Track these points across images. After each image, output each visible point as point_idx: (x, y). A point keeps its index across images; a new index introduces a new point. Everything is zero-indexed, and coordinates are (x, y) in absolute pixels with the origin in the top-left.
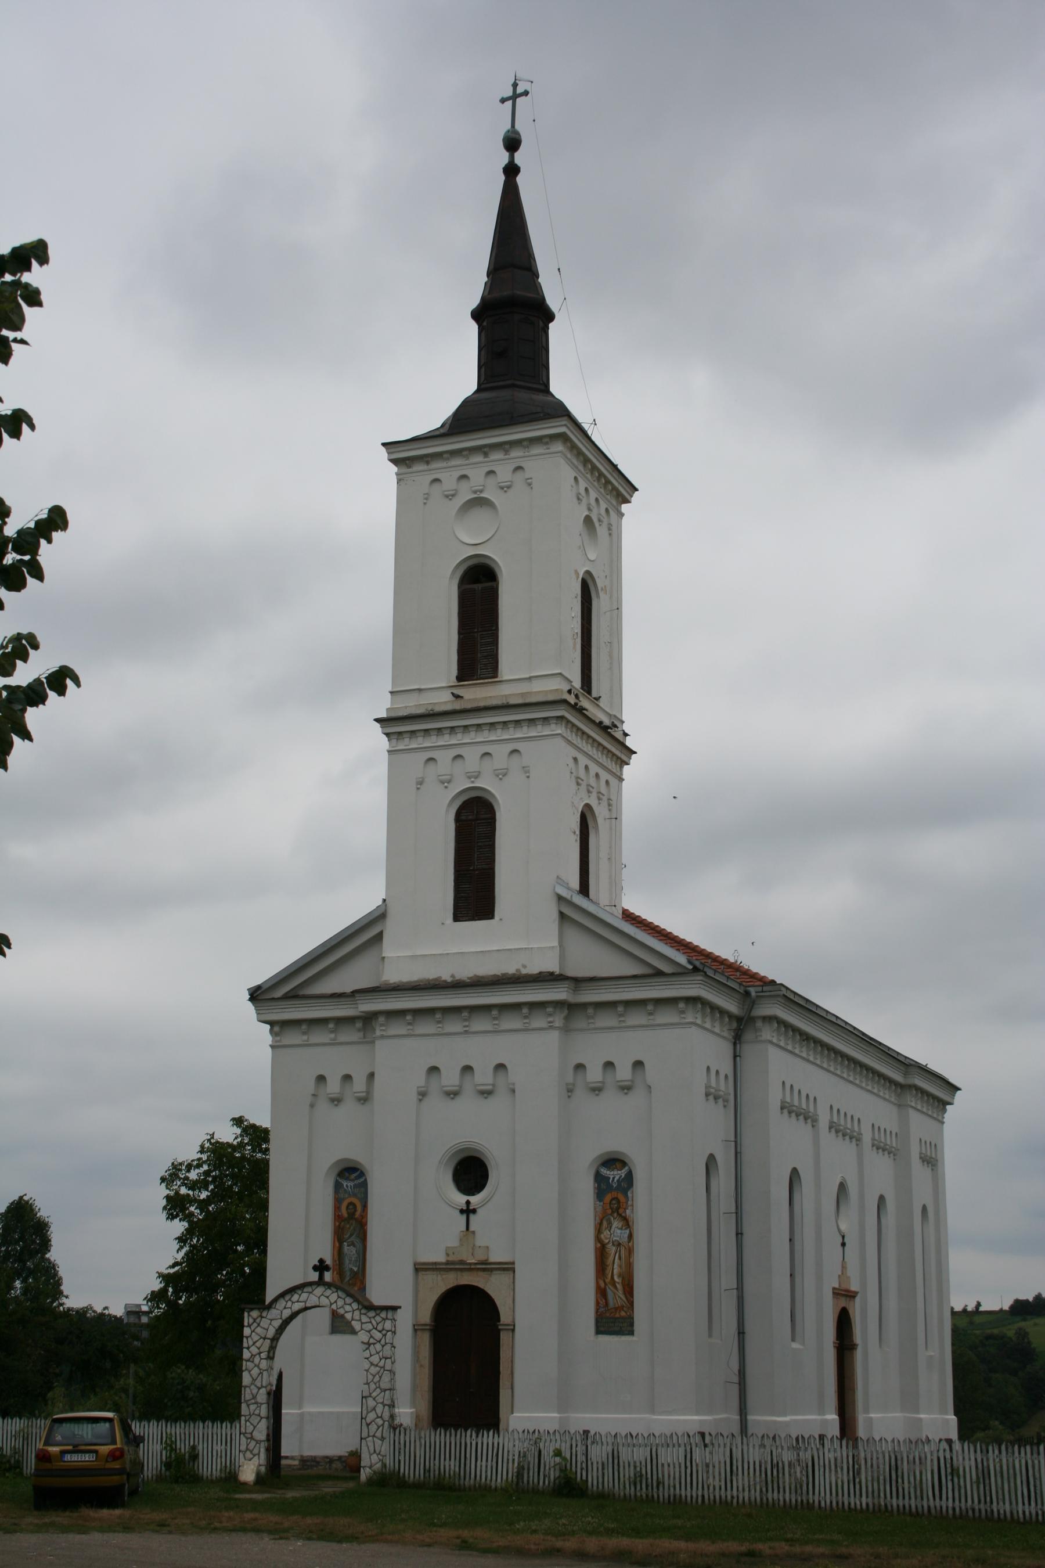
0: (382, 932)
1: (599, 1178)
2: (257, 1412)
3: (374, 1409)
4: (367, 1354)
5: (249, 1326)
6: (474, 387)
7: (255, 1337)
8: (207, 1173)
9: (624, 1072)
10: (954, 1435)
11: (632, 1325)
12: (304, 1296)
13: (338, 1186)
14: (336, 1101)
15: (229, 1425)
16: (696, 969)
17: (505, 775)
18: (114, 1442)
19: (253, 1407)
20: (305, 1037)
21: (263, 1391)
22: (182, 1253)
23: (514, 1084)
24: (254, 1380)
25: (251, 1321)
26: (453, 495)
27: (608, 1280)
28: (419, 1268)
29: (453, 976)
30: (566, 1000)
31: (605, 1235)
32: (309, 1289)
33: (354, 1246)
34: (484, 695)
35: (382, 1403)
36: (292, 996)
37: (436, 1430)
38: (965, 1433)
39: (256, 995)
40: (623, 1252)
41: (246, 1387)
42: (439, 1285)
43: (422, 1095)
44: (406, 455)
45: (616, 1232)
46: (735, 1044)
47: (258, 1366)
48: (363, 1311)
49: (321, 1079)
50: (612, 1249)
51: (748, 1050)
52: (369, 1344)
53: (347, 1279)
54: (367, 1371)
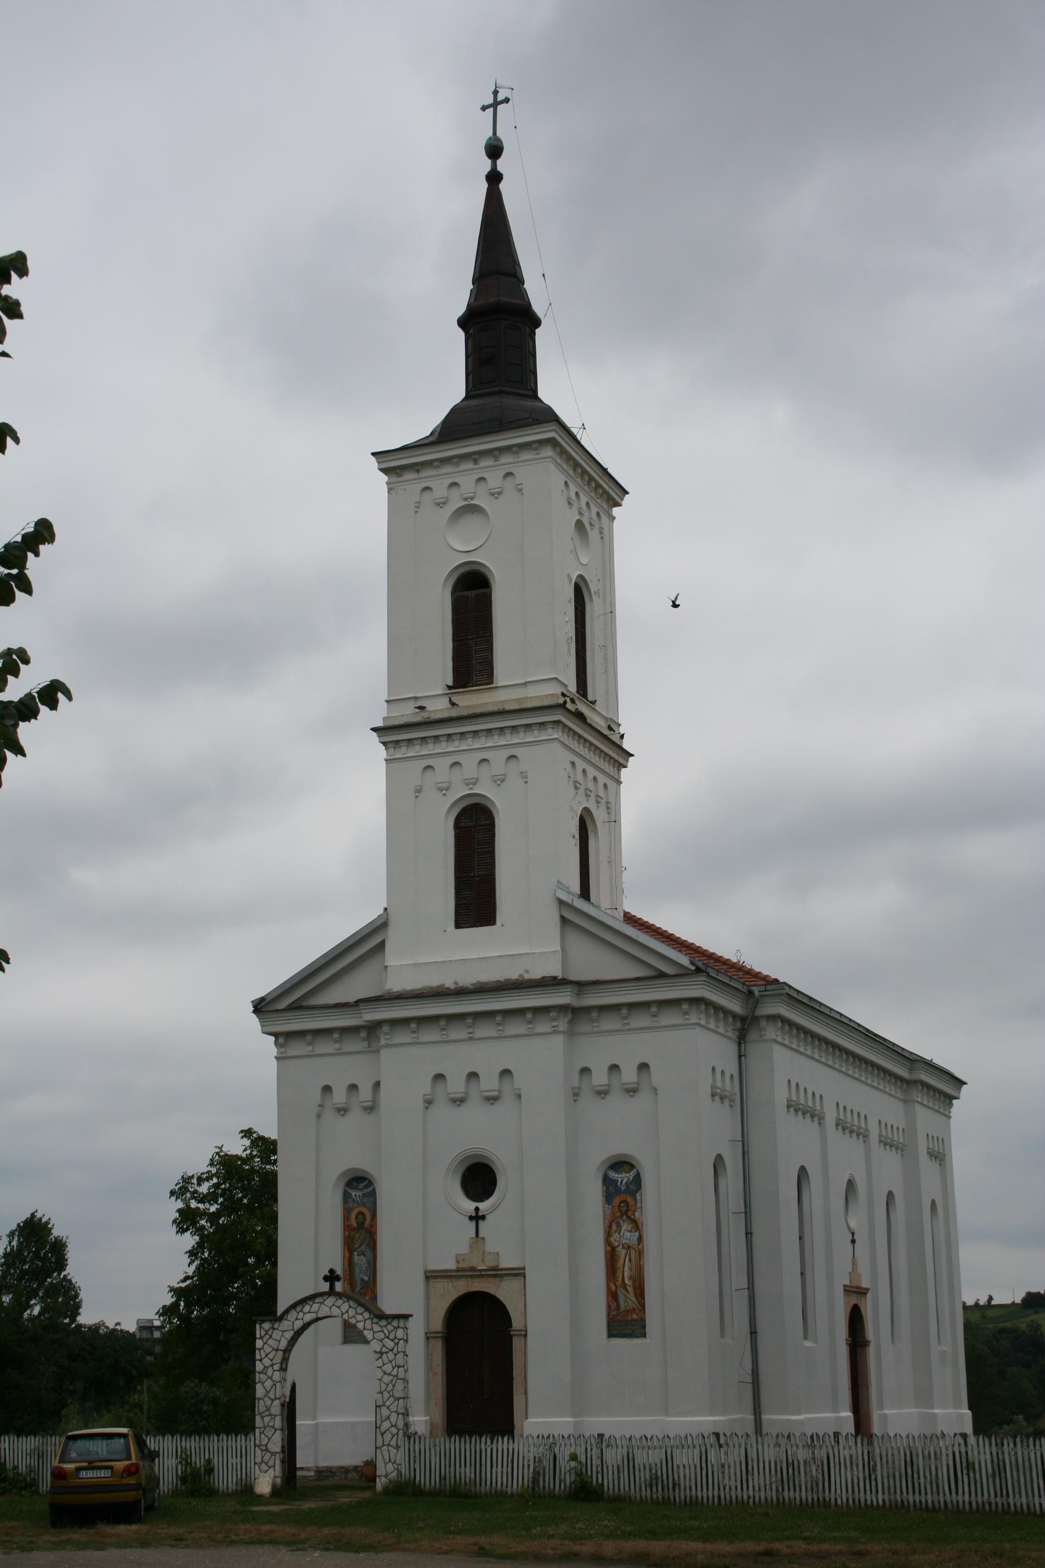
1: (607, 1181)
2: (271, 1424)
3: (388, 1418)
4: (380, 1363)
5: (261, 1338)
6: (462, 394)
7: (268, 1349)
8: (216, 1186)
9: (629, 1075)
10: (969, 1429)
11: (644, 1327)
12: (316, 1307)
13: (346, 1196)
14: (343, 1111)
15: (243, 1438)
16: (698, 970)
17: (503, 781)
18: (129, 1458)
20: (310, 1048)
21: (277, 1403)
22: (193, 1267)
23: (519, 1089)
24: (268, 1392)
25: (263, 1333)
26: (444, 503)
27: (619, 1283)
28: (430, 1276)
29: (456, 983)
30: (569, 1004)
31: (615, 1238)
32: (320, 1300)
34: (479, 702)
35: (396, 1412)
36: (296, 1007)
37: (450, 1438)
38: (981, 1426)
39: (260, 1007)
40: (633, 1255)
41: (259, 1399)
42: (450, 1292)
43: (429, 1102)
44: (396, 464)
45: (626, 1235)
46: (739, 1044)
47: (271, 1378)
48: (375, 1320)
49: (327, 1089)
50: (622, 1252)
51: (754, 1050)
52: (381, 1353)
54: (380, 1380)
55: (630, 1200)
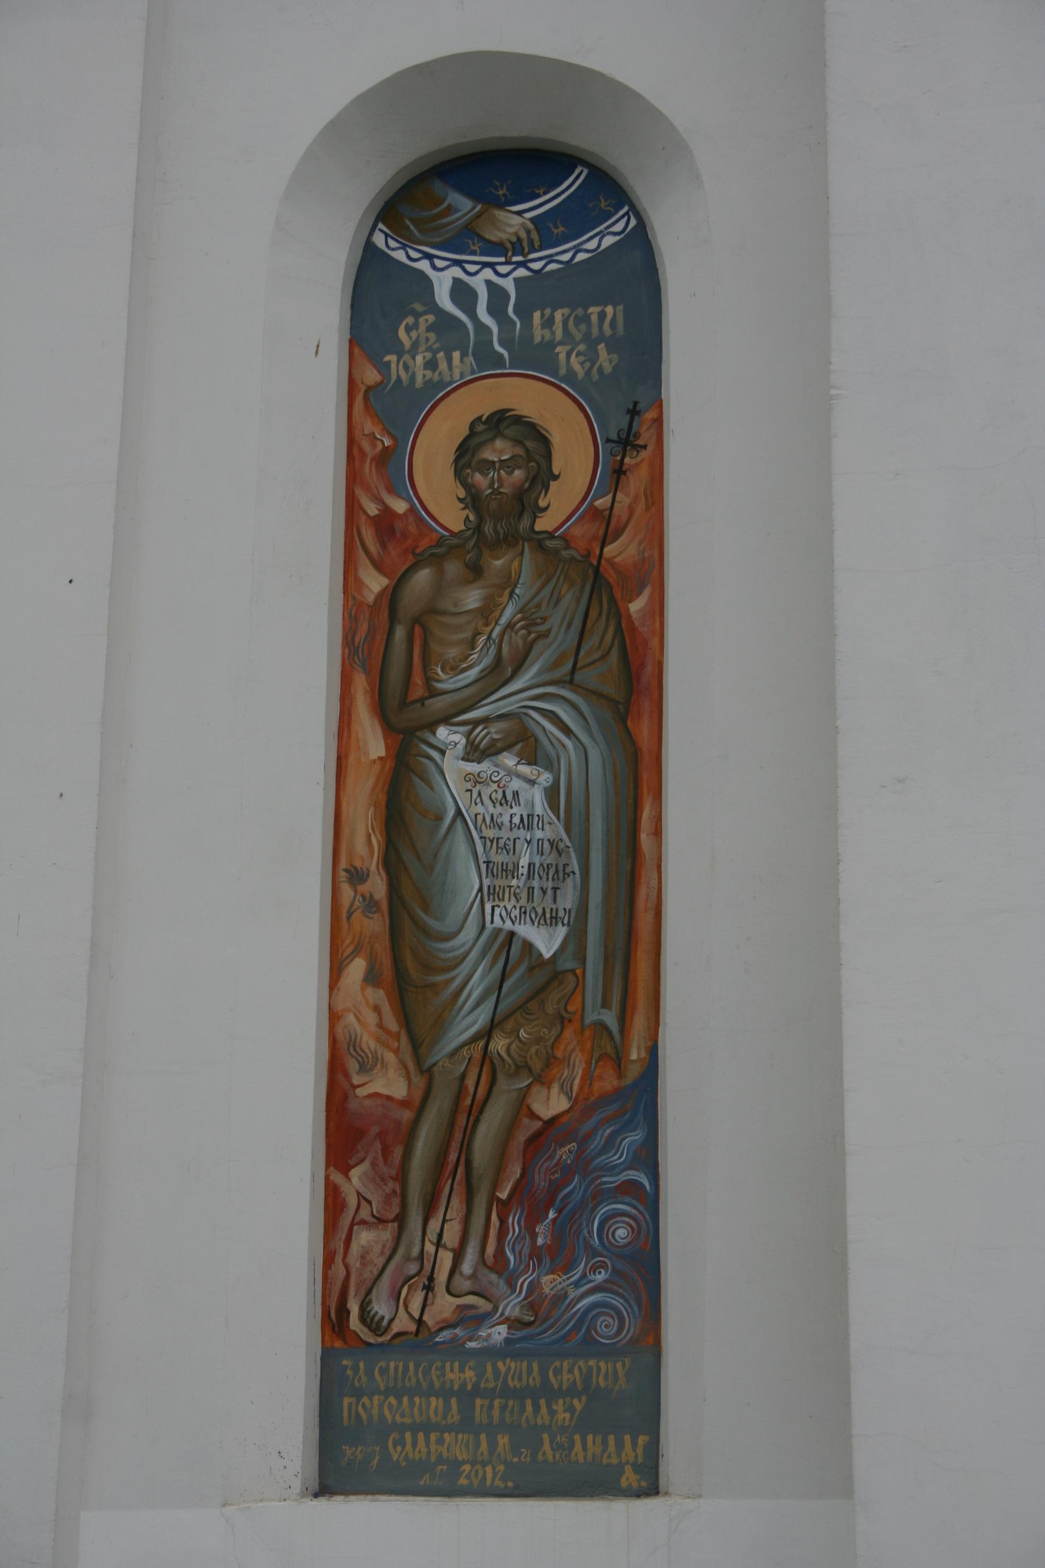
13: (377, 296)
33: (532, 752)
53: (469, 1022)
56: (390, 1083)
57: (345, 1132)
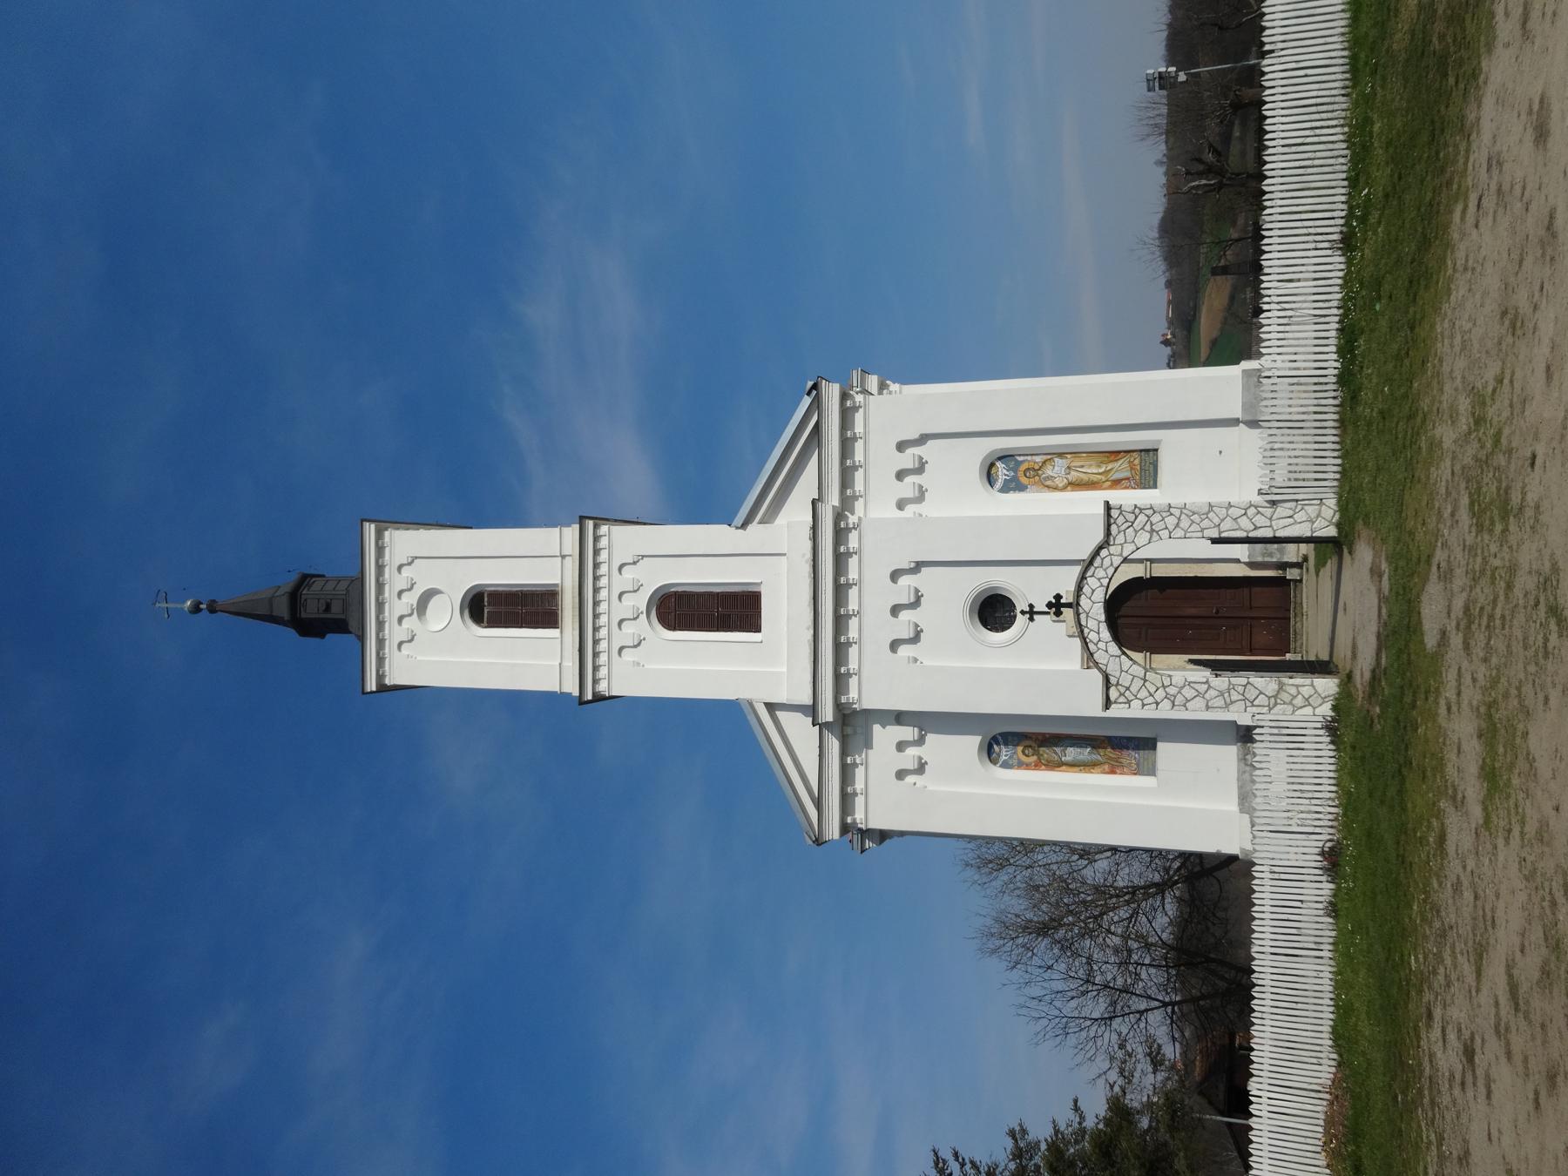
0: (767, 704)
2: (1241, 689)
7: (1143, 694)
9: (907, 460)
12: (1092, 624)
13: (1006, 765)
19: (1235, 696)
24: (1199, 694)
32: (1083, 617)
50: (1074, 476)
52: (1153, 530)
55: (1025, 466)
56: (1106, 767)
57: (1113, 772)
